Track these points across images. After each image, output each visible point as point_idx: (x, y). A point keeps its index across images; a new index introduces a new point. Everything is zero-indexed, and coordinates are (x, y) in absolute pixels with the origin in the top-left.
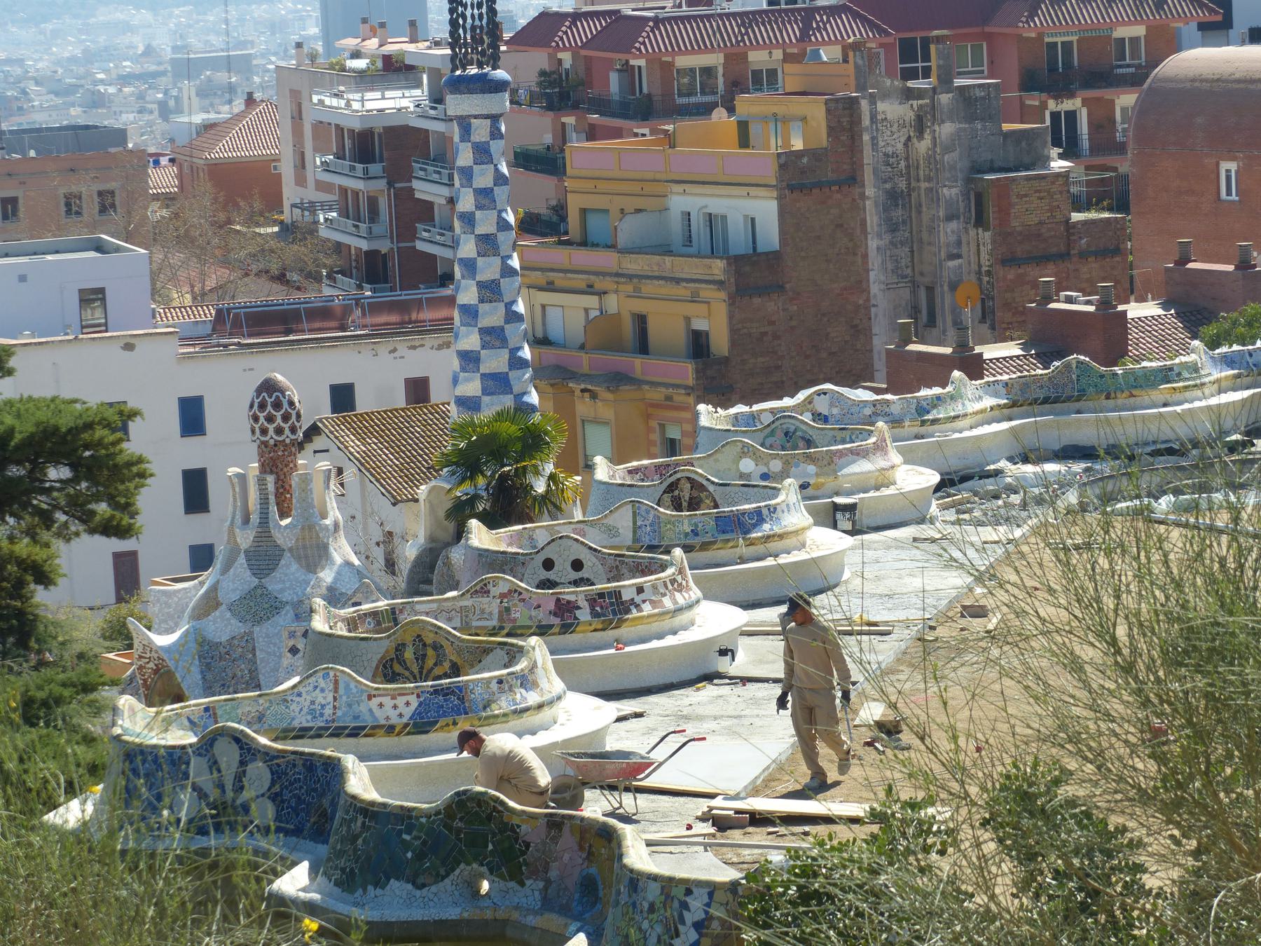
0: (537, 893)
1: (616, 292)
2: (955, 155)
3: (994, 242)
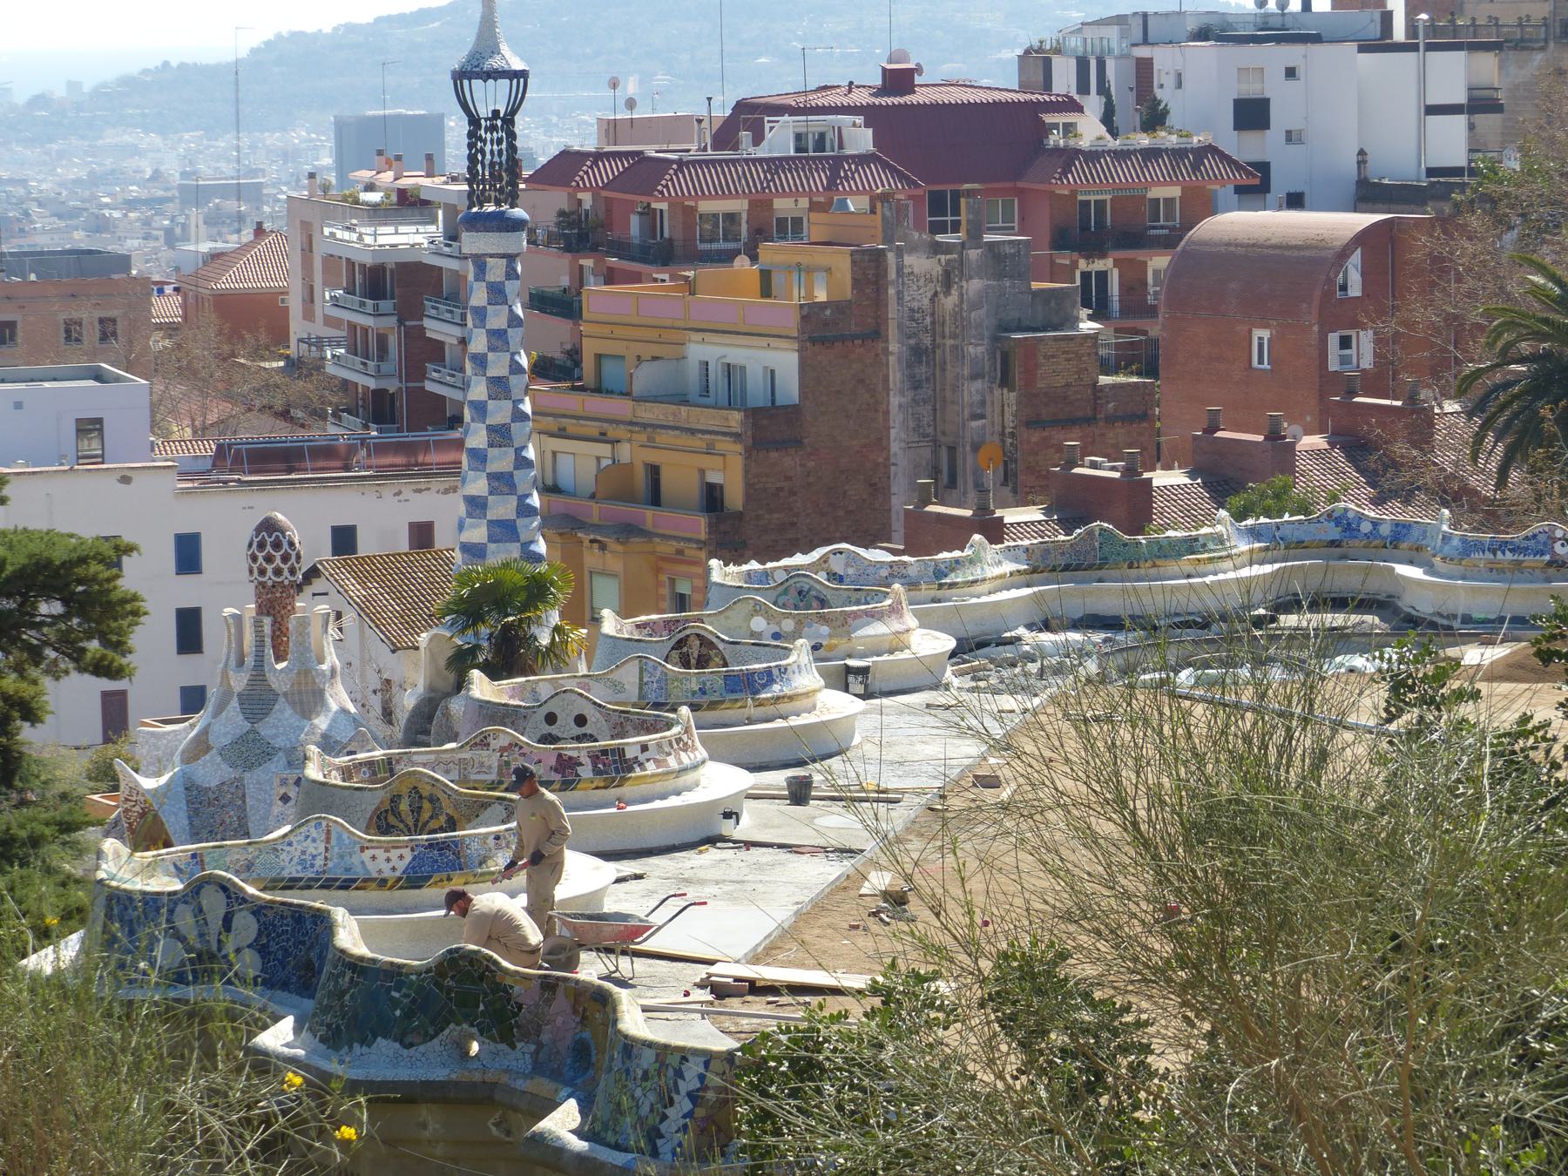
0: (527, 1056)
1: (629, 440)
2: (982, 312)
3: (1019, 403)
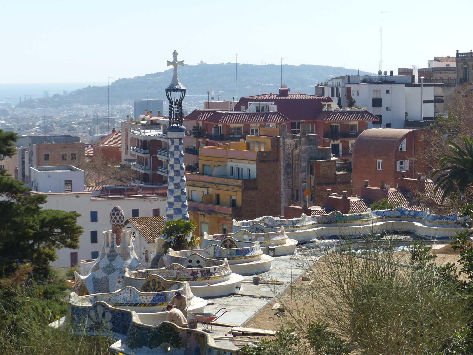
1: (212, 187)
2: (305, 154)
3: (315, 179)
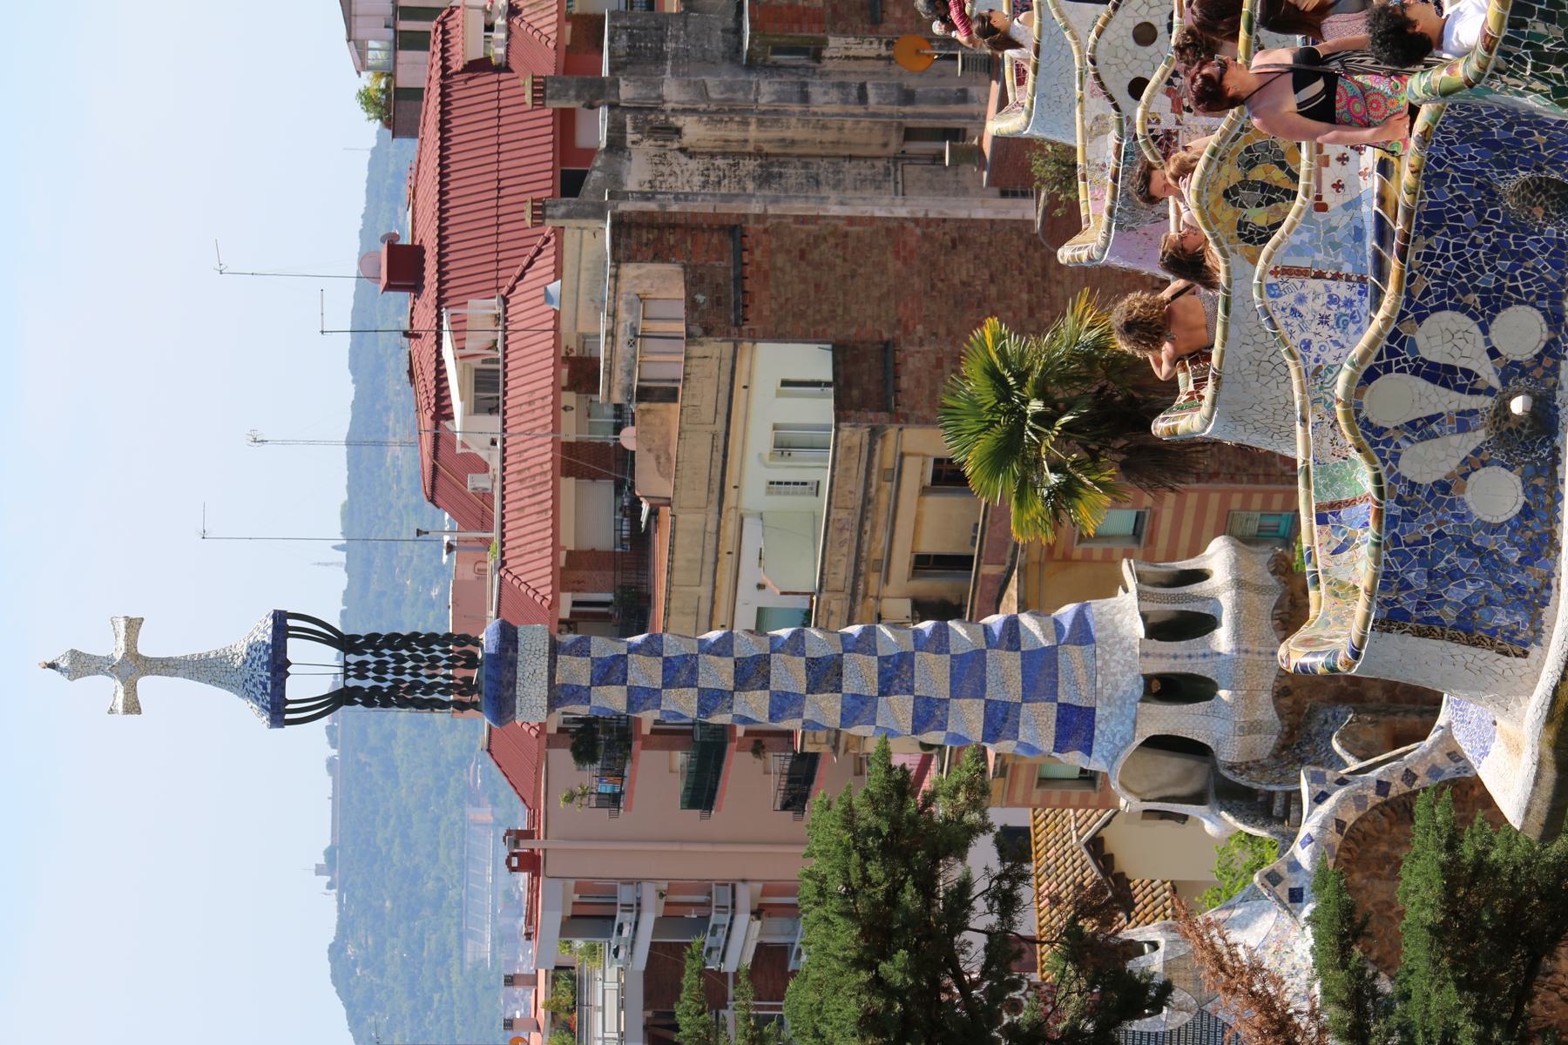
2: (711, 82)
3: (844, 33)
